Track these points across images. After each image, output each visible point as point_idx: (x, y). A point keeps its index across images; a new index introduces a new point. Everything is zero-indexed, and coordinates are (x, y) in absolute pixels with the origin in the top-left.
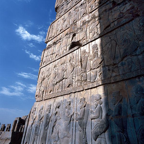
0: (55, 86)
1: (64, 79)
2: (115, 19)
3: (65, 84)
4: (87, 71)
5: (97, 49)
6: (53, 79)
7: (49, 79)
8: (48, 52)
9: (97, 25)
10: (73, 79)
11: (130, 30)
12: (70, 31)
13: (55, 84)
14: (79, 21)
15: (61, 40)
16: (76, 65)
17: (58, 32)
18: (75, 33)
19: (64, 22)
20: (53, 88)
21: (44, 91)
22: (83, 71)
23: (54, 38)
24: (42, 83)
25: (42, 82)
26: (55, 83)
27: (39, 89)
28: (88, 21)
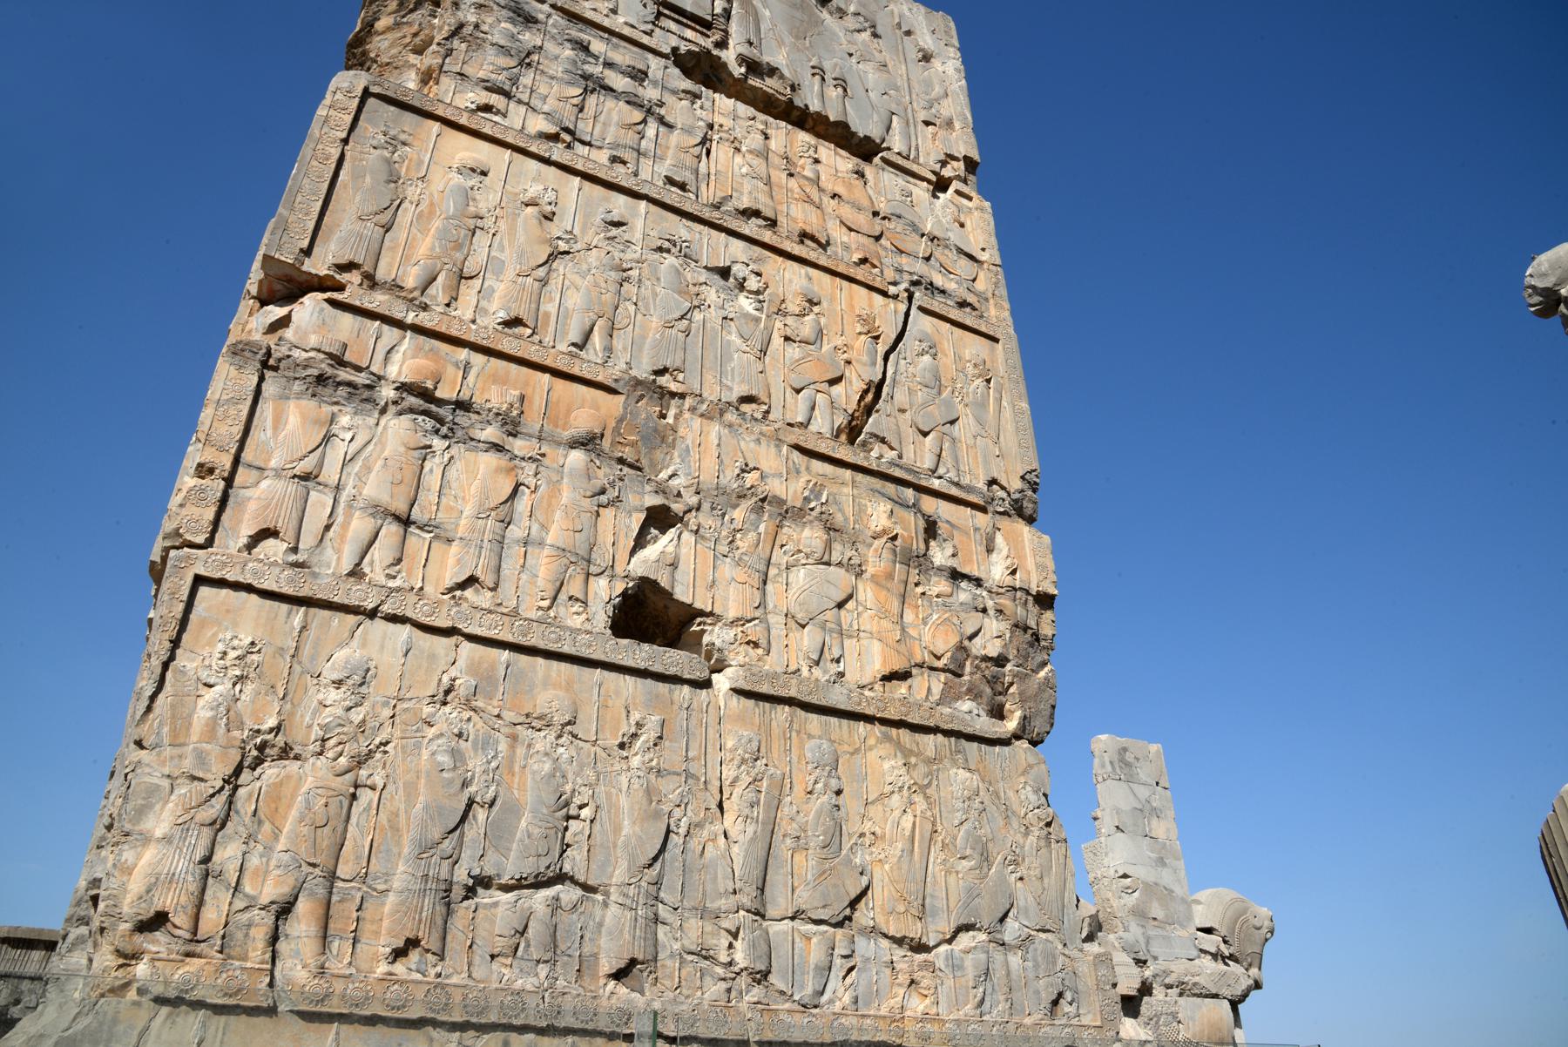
0: (463, 910)
1: (561, 878)
2: (935, 656)
3: (588, 936)
4: (771, 912)
5: (839, 793)
6: (436, 834)
7: (366, 796)
8: (328, 438)
9: (840, 605)
10: (656, 919)
11: (991, 789)
12: (616, 430)
13: (458, 892)
14: (714, 429)
15: (519, 446)
16: (678, 813)
17: (469, 292)
18: (677, 507)
19: (553, 256)
20: (439, 921)
21: (285, 909)
22: (745, 900)
23: (419, 330)
24: (236, 787)
25: (238, 771)
26: (461, 875)
27: (199, 854)
28: (781, 502)
